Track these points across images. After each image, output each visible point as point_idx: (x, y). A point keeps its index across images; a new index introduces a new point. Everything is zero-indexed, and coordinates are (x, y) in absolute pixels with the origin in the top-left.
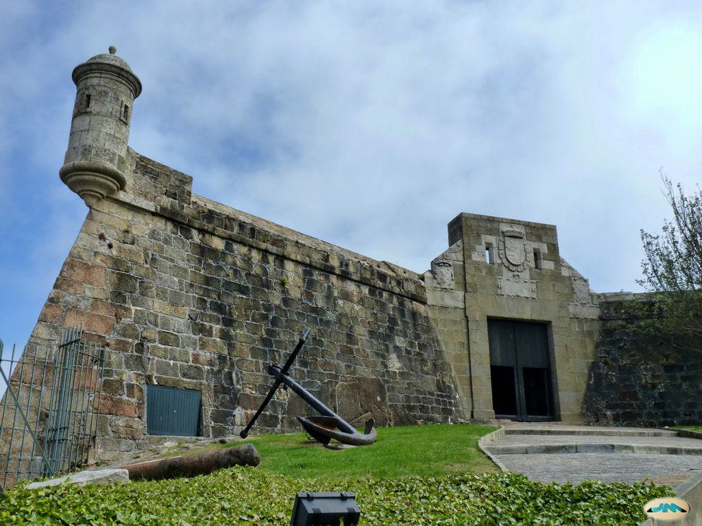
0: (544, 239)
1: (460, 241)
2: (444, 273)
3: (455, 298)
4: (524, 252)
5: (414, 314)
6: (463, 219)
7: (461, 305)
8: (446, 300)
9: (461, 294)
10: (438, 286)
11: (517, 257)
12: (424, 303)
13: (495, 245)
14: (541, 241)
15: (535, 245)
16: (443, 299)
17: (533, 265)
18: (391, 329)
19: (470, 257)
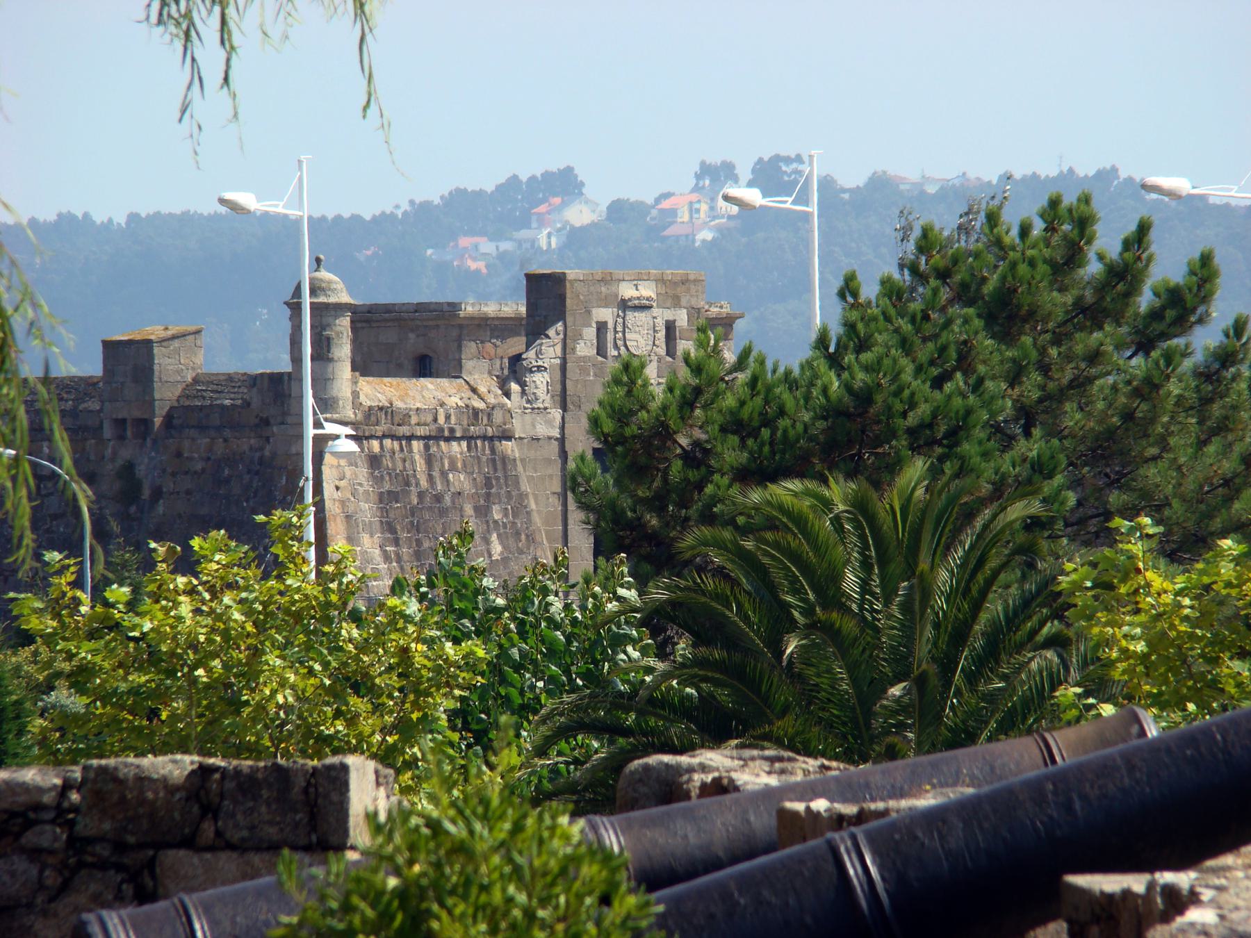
0: (684, 302)
1: (560, 326)
2: (538, 382)
3: (549, 423)
4: (651, 332)
5: (504, 459)
6: (568, 285)
7: (556, 433)
8: (538, 426)
9: (556, 414)
10: (529, 406)
11: (642, 342)
12: (509, 438)
13: (610, 325)
14: (680, 307)
15: (669, 315)
16: (534, 426)
17: (662, 351)
18: (488, 495)
19: (574, 349)
